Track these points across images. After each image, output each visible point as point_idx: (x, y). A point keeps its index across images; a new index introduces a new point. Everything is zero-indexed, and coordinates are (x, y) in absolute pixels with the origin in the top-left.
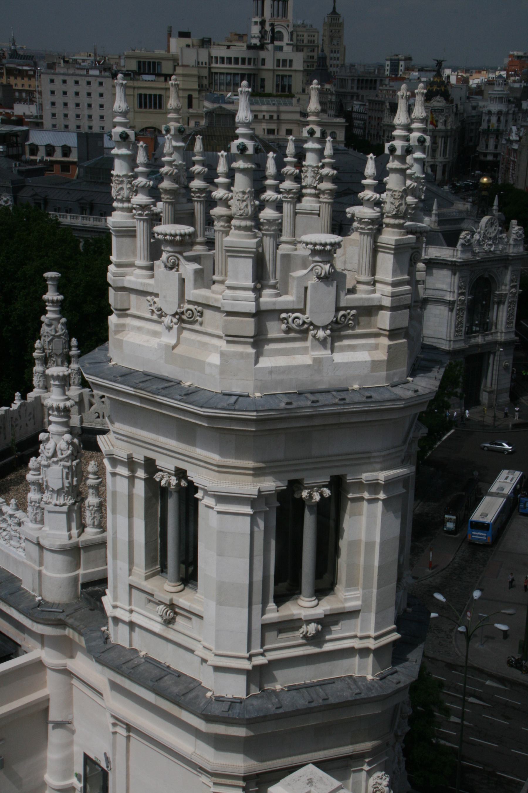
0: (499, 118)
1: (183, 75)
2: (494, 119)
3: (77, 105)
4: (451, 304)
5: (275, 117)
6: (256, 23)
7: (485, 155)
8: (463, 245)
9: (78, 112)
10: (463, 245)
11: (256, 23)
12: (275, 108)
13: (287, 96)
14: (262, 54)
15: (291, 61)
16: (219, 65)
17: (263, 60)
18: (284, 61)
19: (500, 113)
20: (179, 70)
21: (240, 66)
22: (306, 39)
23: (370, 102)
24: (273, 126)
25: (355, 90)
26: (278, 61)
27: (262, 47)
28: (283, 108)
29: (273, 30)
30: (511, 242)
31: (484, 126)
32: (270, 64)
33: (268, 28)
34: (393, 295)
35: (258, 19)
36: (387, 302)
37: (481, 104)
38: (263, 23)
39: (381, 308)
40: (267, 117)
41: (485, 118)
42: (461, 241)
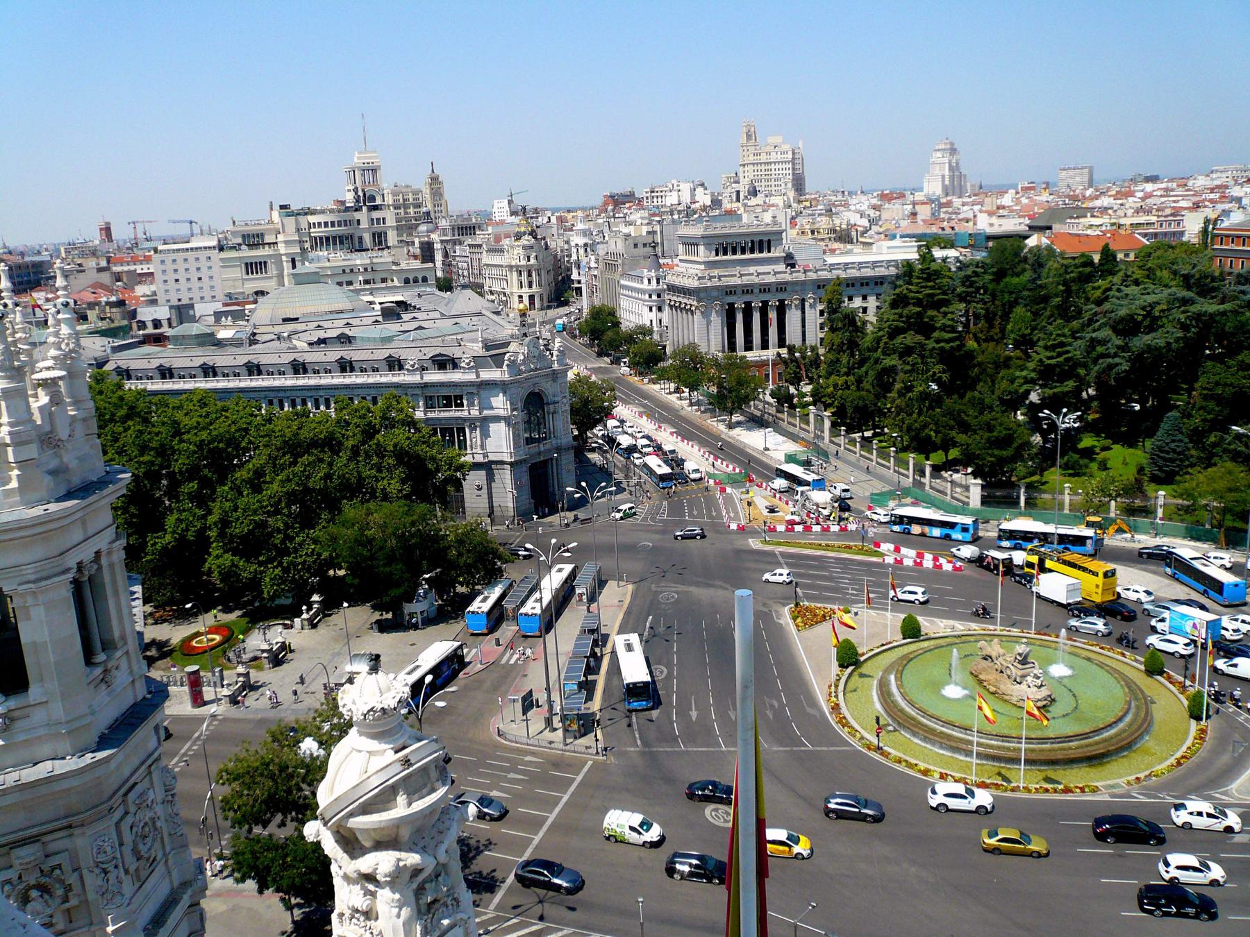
0: (586, 250)
1: (285, 242)
2: (582, 251)
3: (188, 279)
4: (507, 420)
5: (369, 270)
6: (349, 190)
7: (579, 282)
8: (508, 365)
9: (189, 286)
10: (508, 365)
11: (349, 190)
12: (368, 261)
13: (383, 249)
14: (357, 215)
15: (384, 219)
16: (317, 230)
17: (359, 221)
18: (378, 220)
19: (586, 245)
20: (281, 238)
21: (336, 228)
22: (411, 197)
23: (470, 245)
24: (369, 277)
25: (456, 237)
26: (372, 220)
27: (358, 209)
28: (375, 261)
29: (364, 195)
30: (555, 358)
31: (574, 257)
32: (364, 224)
33: (361, 194)
34: (10, 433)
35: (352, 188)
36: (8, 440)
37: (571, 238)
38: (356, 190)
39: (8, 445)
40: (361, 270)
41: (574, 250)
42: (506, 363)
